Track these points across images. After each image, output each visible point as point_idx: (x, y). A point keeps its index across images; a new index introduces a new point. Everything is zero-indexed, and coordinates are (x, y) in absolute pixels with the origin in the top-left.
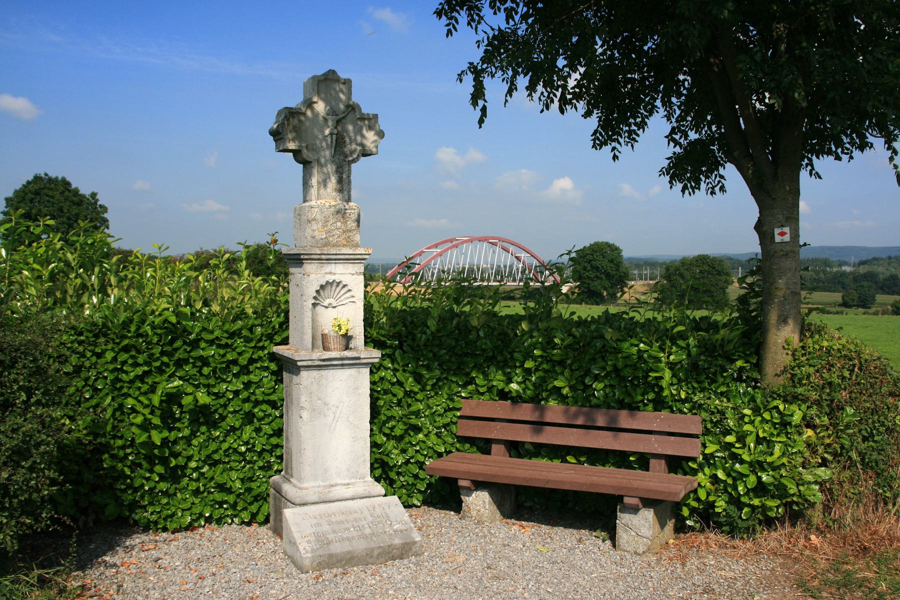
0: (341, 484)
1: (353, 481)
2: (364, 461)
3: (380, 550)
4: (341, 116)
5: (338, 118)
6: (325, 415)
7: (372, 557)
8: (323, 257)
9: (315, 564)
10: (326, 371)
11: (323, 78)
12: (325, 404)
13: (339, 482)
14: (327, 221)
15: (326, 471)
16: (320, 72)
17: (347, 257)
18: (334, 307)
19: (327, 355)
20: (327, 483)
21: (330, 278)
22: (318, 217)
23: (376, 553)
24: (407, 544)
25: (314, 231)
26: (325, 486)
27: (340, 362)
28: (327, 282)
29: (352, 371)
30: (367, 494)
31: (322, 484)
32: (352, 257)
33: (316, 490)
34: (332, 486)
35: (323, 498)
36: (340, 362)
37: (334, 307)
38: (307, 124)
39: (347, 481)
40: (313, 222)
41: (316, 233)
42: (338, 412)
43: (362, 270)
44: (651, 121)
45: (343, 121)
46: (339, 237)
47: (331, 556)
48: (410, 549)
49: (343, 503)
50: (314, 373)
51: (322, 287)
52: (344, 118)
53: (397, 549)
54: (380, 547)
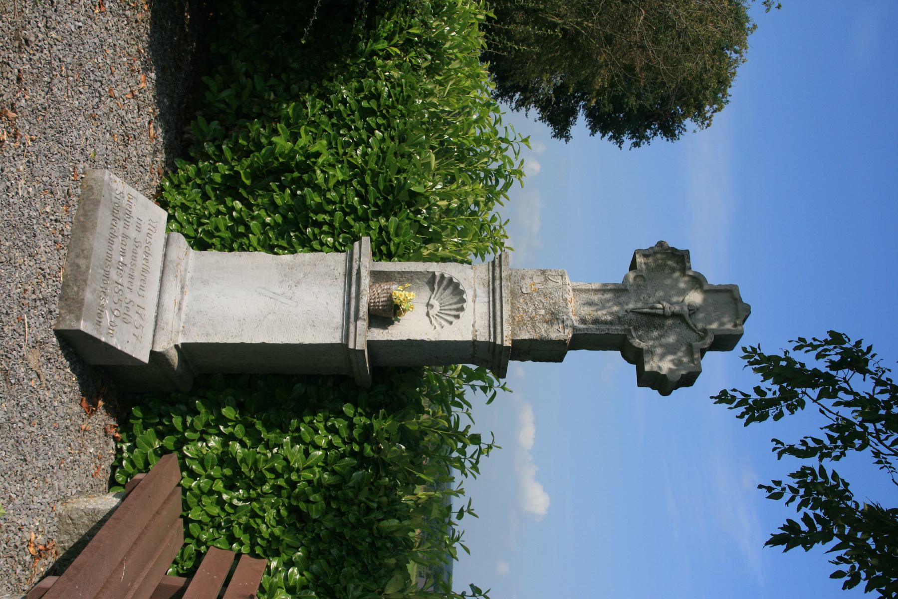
0: (182, 299)
1: (183, 317)
2: (207, 335)
3: (84, 267)
4: (690, 322)
5: (687, 316)
6: (282, 281)
7: (78, 256)
8: (498, 282)
9: (92, 183)
10: (342, 284)
11: (737, 297)
12: (298, 283)
13: (186, 298)
14: (545, 296)
15: (205, 282)
16: (746, 297)
17: (498, 314)
18: (428, 314)
19: (366, 281)
20: (187, 283)
21: (468, 296)
22: (551, 284)
23: (82, 262)
24: (80, 309)
25: (531, 278)
26: (185, 278)
27: (353, 295)
28: (463, 292)
29: (338, 317)
30: (161, 324)
31: (189, 275)
32: (498, 319)
33: (183, 263)
34: (182, 288)
35: (170, 266)
36: (353, 295)
37: (428, 314)
38: (668, 282)
39: (184, 304)
40: (542, 278)
41: (528, 281)
42: (283, 300)
43: (481, 338)
44: (818, 547)
45: (684, 326)
46: (525, 311)
47: (97, 203)
48: (70, 312)
49: (157, 288)
50: (341, 269)
51: (457, 285)
52: (688, 325)
53: (78, 293)
54: (88, 268)
